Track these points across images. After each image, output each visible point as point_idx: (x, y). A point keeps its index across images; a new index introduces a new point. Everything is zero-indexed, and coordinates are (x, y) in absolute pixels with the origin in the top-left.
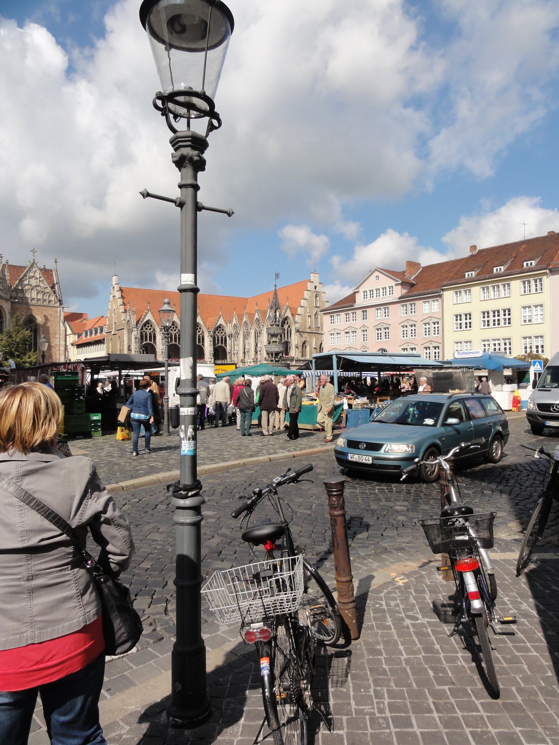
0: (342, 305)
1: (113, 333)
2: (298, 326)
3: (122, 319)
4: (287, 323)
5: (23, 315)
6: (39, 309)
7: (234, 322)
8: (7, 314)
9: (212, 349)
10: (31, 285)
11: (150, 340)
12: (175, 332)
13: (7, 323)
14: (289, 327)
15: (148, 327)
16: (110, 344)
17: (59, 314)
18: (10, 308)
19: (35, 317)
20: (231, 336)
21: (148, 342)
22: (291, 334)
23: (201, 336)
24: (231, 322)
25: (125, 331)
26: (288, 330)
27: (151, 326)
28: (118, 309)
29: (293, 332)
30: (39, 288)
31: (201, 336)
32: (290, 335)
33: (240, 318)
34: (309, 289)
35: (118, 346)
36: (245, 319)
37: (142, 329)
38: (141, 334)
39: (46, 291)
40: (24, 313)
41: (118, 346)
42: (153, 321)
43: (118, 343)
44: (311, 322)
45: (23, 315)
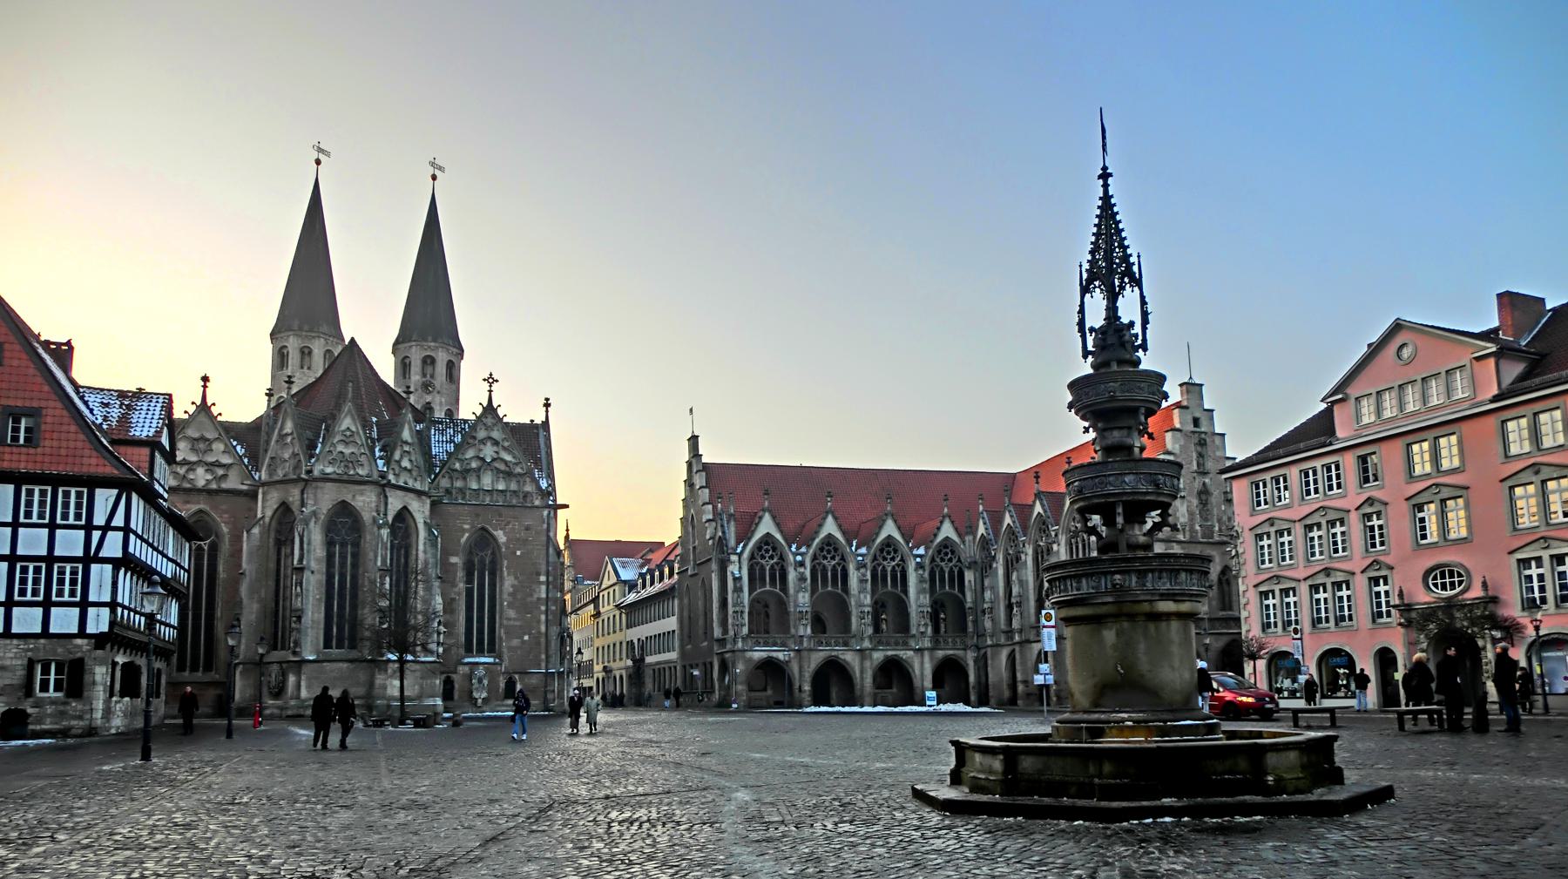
0: (1292, 448)
5: (464, 531)
7: (981, 530)
8: (421, 527)
9: (926, 600)
10: (483, 459)
13: (421, 547)
16: (686, 601)
18: (427, 513)
20: (972, 565)
23: (898, 569)
24: (972, 530)
25: (714, 566)
27: (774, 549)
28: (700, 513)
30: (502, 467)
31: (898, 569)
33: (996, 520)
34: (1178, 426)
36: (1008, 520)
37: (752, 557)
39: (518, 470)
42: (778, 536)
44: (1191, 514)
45: (464, 531)
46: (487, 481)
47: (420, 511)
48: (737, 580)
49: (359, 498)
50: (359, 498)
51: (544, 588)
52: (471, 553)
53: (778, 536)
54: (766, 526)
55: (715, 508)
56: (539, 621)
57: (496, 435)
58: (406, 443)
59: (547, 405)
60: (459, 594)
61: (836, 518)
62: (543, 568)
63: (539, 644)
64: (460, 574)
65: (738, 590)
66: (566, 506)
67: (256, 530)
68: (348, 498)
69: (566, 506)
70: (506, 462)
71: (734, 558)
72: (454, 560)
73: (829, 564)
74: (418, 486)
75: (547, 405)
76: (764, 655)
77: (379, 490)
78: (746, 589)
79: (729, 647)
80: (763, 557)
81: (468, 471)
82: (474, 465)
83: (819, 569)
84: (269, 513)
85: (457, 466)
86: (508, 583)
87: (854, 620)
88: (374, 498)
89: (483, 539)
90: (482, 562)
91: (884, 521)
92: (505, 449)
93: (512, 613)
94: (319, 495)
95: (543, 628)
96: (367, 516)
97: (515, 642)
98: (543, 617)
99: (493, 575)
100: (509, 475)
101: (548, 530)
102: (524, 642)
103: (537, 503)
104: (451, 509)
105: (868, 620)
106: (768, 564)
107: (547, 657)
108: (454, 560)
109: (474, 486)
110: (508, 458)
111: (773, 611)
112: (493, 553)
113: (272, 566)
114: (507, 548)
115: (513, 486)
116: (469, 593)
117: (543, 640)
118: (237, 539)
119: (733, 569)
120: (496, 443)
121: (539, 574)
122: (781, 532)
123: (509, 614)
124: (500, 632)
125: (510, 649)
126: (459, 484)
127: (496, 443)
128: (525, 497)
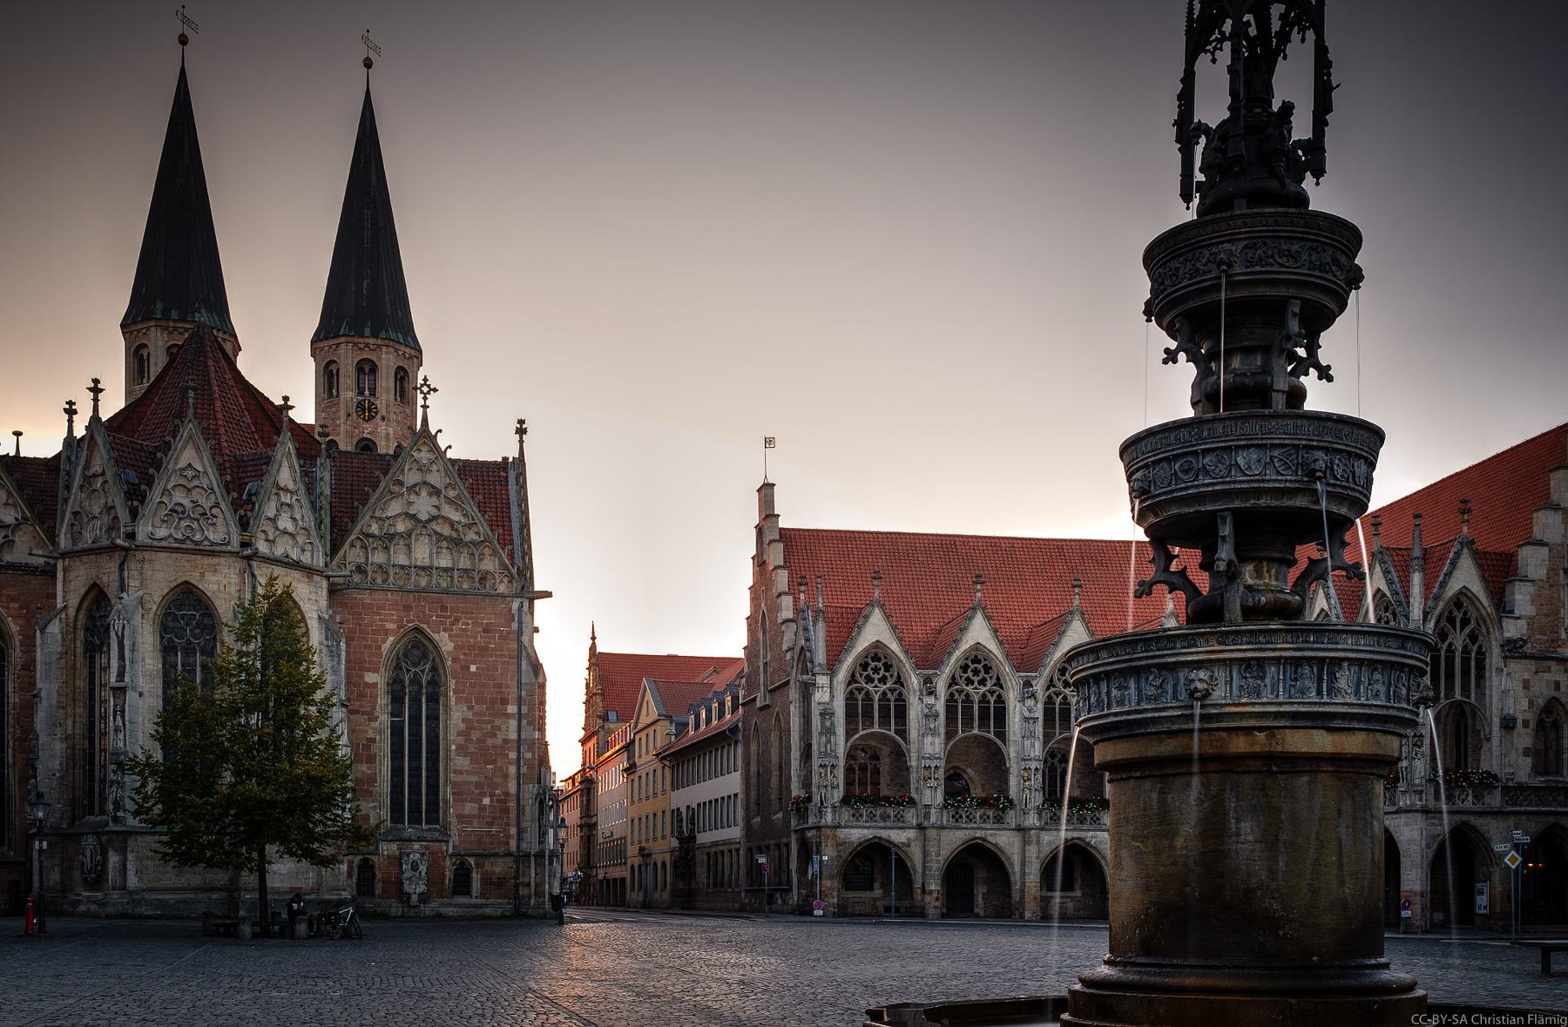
1: (758, 704)
2: (1513, 629)
3: (785, 648)
4: (1465, 622)
5: (387, 633)
6: (444, 608)
11: (885, 720)
12: (983, 689)
14: (1473, 637)
15: (876, 670)
17: (515, 626)
18: (324, 602)
19: (431, 640)
21: (876, 729)
22: (1481, 668)
25: (794, 693)
26: (1466, 651)
27: (888, 667)
28: (778, 608)
29: (1495, 657)
32: (1481, 676)
35: (774, 752)
37: (852, 679)
38: (850, 699)
39: (471, 536)
40: (391, 626)
41: (774, 752)
42: (894, 646)
43: (774, 737)
45: (387, 633)
46: (422, 552)
47: (311, 600)
48: (827, 713)
49: (210, 577)
50: (210, 577)
51: (513, 723)
52: (398, 667)
53: (894, 646)
54: (875, 630)
55: (796, 600)
56: (506, 776)
57: (436, 478)
58: (286, 490)
59: (521, 431)
60: (380, 732)
61: (988, 618)
62: (513, 693)
63: (507, 811)
64: (383, 701)
65: (829, 731)
66: (548, 595)
67: (55, 628)
68: (194, 578)
69: (548, 595)
70: (452, 524)
71: (822, 680)
72: (370, 678)
73: (976, 692)
74: (306, 559)
75: (521, 431)
76: (868, 833)
77: (243, 564)
78: (840, 730)
79: (812, 820)
80: (869, 680)
81: (392, 537)
82: (401, 527)
83: (960, 698)
84: (74, 601)
85: (374, 529)
86: (456, 715)
87: (1013, 781)
88: (234, 579)
89: (417, 647)
90: (416, 681)
91: (1068, 623)
92: (450, 501)
93: (462, 762)
94: (148, 573)
95: (512, 788)
96: (225, 608)
97: (470, 808)
98: (512, 770)
99: (434, 699)
100: (456, 543)
101: (520, 632)
102: (482, 808)
103: (502, 589)
104: (366, 597)
105: (1037, 781)
106: (876, 691)
107: (520, 831)
108: (370, 678)
109: (402, 559)
110: (455, 516)
111: (885, 765)
112: (434, 669)
113: (81, 684)
114: (455, 660)
115: (465, 562)
116: (397, 731)
117: (512, 805)
118: (29, 644)
119: (820, 696)
120: (435, 492)
121: (505, 702)
122: (900, 640)
123: (457, 765)
124: (446, 792)
125: (461, 818)
126: (378, 557)
127: (435, 492)
128: (483, 579)
